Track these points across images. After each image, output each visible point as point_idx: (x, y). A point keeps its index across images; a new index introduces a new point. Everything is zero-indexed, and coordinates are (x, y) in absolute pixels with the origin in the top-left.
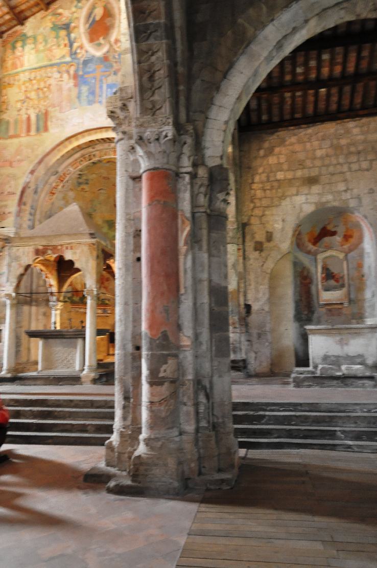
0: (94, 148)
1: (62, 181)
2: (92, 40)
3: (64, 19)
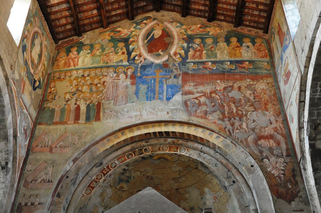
0: (147, 142)
1: (104, 175)
2: (150, 51)
3: (123, 35)
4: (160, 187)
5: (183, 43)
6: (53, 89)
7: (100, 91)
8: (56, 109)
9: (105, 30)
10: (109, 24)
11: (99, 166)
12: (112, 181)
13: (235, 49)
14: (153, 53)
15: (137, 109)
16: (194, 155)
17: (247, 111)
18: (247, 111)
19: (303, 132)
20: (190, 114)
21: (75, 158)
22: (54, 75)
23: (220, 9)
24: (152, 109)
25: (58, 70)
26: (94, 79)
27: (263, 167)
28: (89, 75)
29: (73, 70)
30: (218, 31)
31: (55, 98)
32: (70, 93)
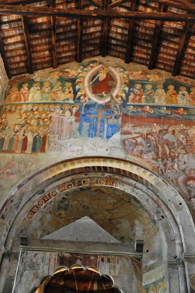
0: (86, 175)
1: (45, 201)
2: (94, 92)
3: (70, 75)
4: (95, 217)
5: (124, 87)
6: (4, 120)
7: (47, 125)
8: (6, 138)
9: (55, 70)
10: (58, 64)
11: (41, 193)
12: (51, 208)
13: (172, 96)
14: (97, 94)
15: (79, 144)
16: (128, 190)
17: (179, 154)
18: (179, 154)
20: (127, 152)
21: (20, 185)
22: (6, 107)
23: (161, 58)
24: (93, 146)
25: (10, 103)
26: (42, 114)
27: (191, 206)
28: (38, 110)
29: (23, 104)
30: (158, 79)
31: (5, 128)
32: (19, 124)
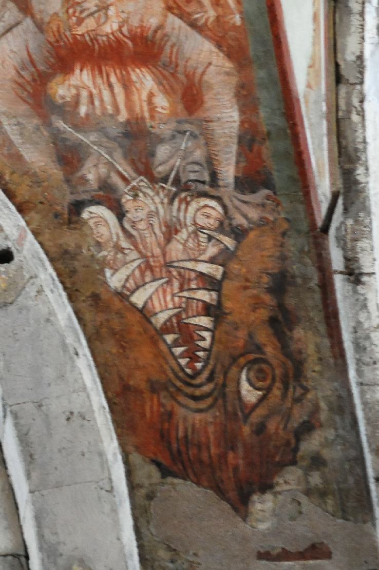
19: (355, 20)
